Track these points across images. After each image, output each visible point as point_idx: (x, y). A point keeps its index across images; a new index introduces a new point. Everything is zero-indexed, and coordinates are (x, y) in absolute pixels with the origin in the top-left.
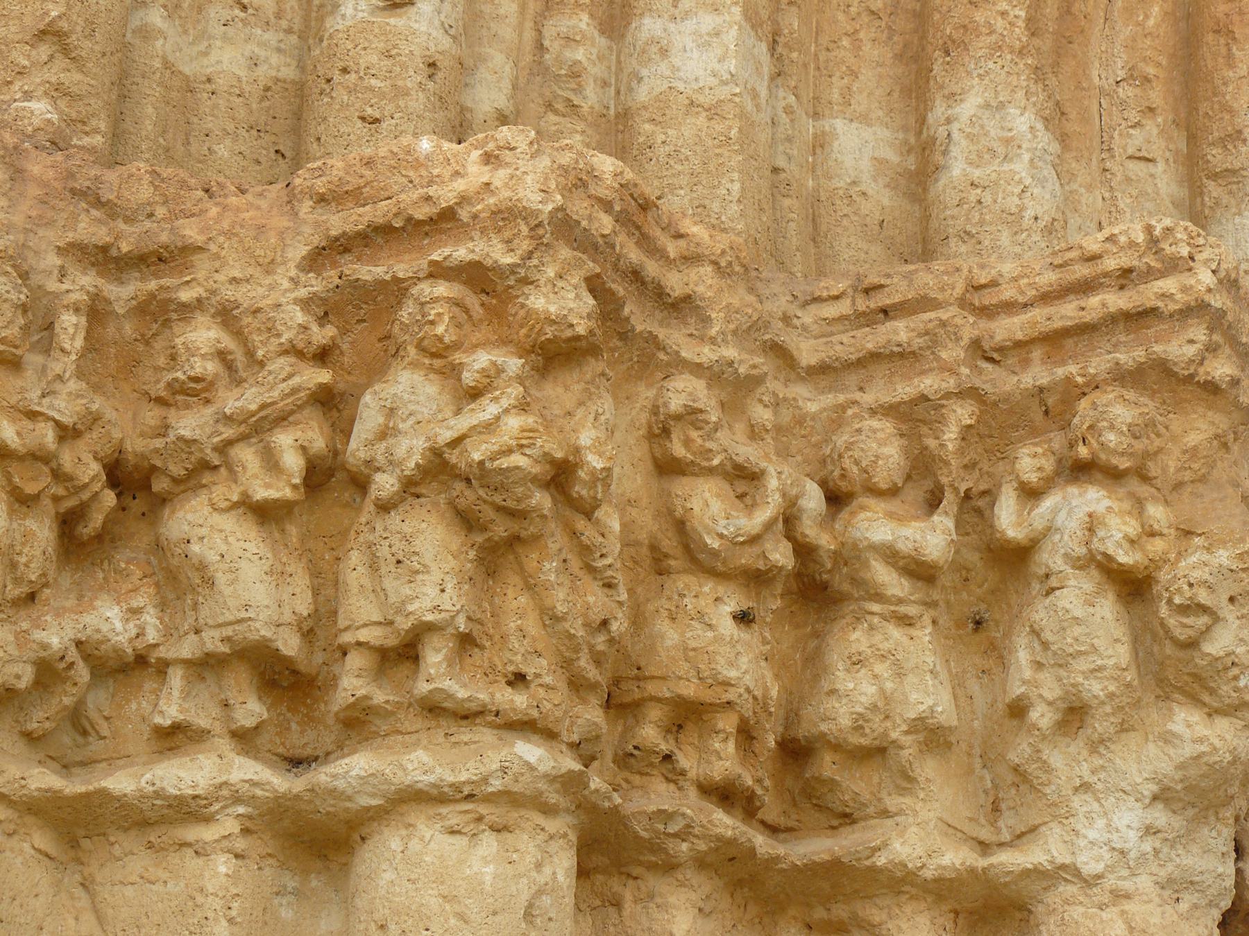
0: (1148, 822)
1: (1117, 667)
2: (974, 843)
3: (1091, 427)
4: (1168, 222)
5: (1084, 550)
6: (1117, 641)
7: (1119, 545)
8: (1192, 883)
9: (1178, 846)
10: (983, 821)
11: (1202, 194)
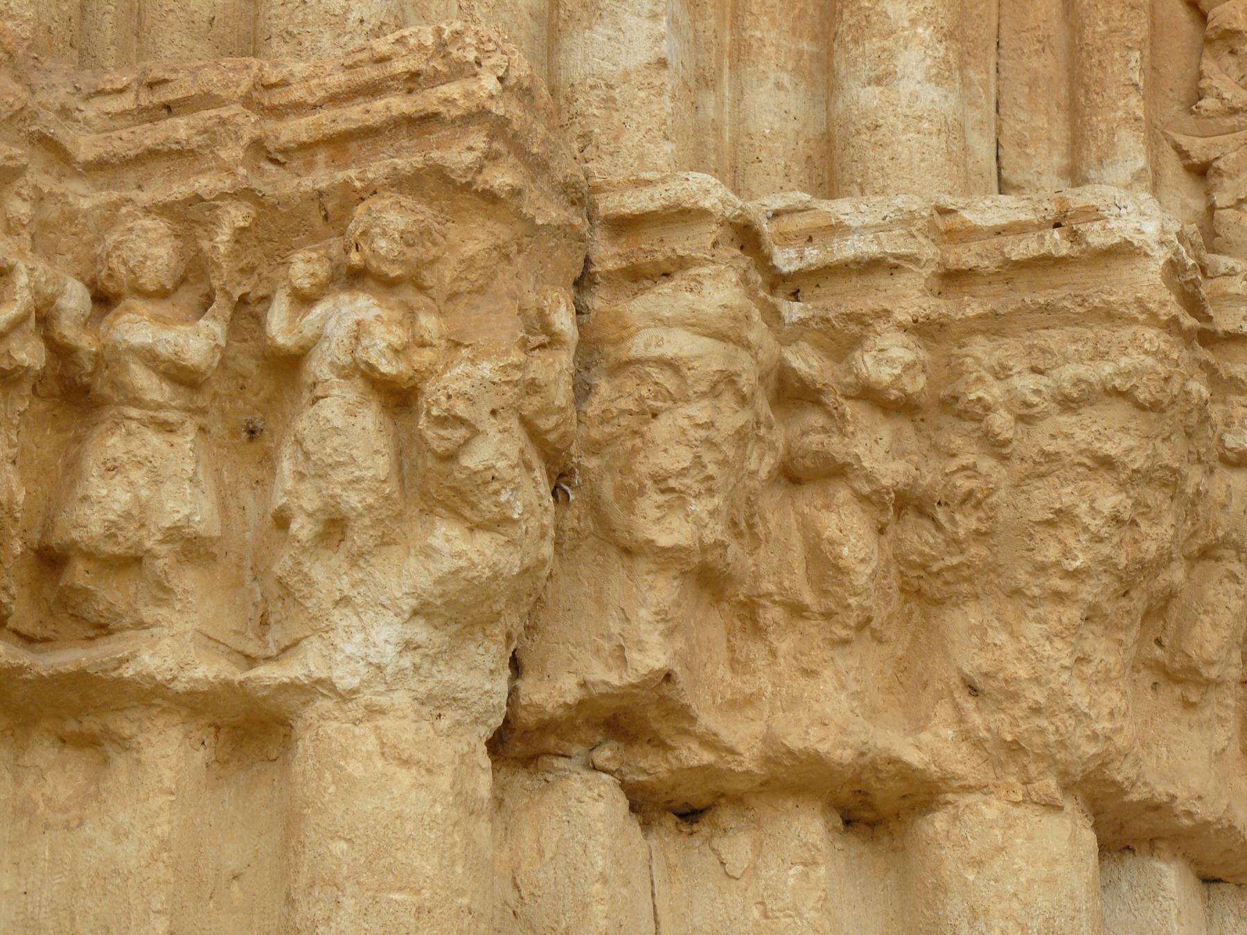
0: (407, 637)
1: (375, 478)
2: (239, 657)
3: (364, 233)
4: (458, 25)
5: (349, 359)
6: (377, 452)
7: (382, 354)
8: (455, 699)
9: (440, 662)
10: (250, 634)
11: (558, 6)
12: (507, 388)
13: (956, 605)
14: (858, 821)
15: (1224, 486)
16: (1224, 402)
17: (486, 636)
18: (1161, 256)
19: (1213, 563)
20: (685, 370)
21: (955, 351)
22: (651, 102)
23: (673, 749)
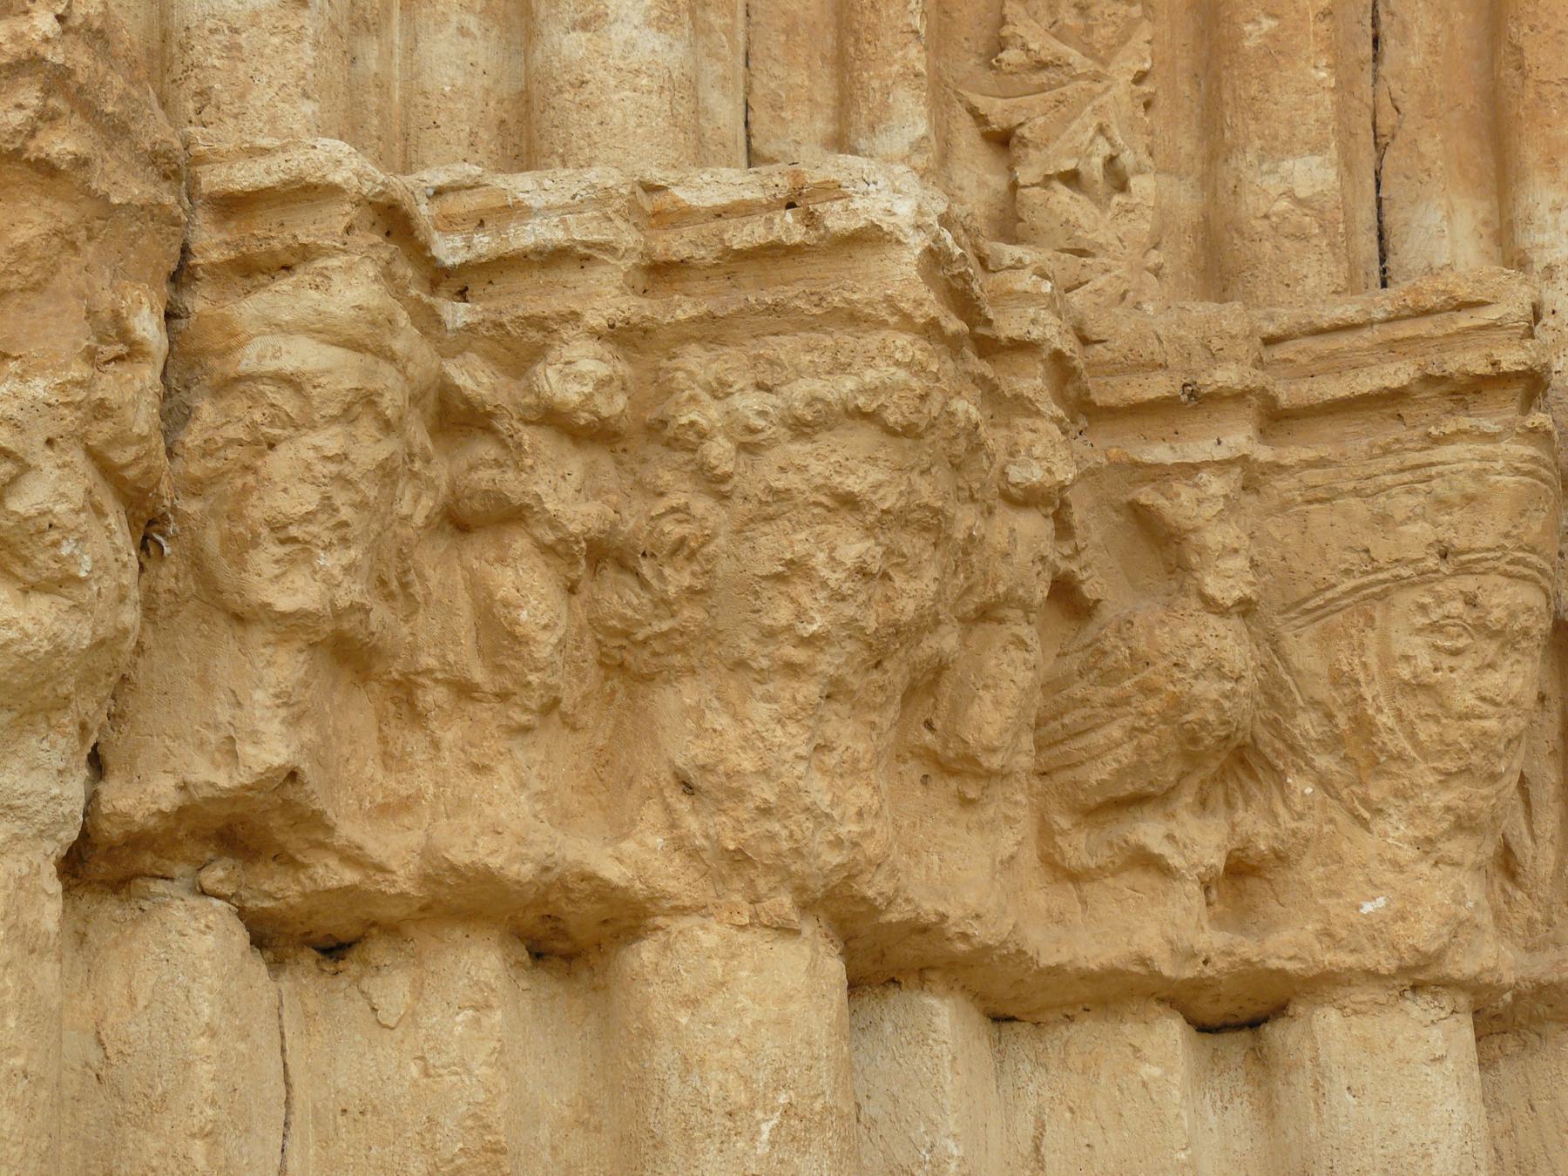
8: (10, 807)
12: (66, 412)
13: (668, 681)
14: (552, 952)
15: (1006, 531)
16: (1008, 426)
17: (50, 727)
18: (917, 243)
19: (995, 626)
20: (309, 388)
21: (664, 363)
22: (286, 50)
23: (305, 866)
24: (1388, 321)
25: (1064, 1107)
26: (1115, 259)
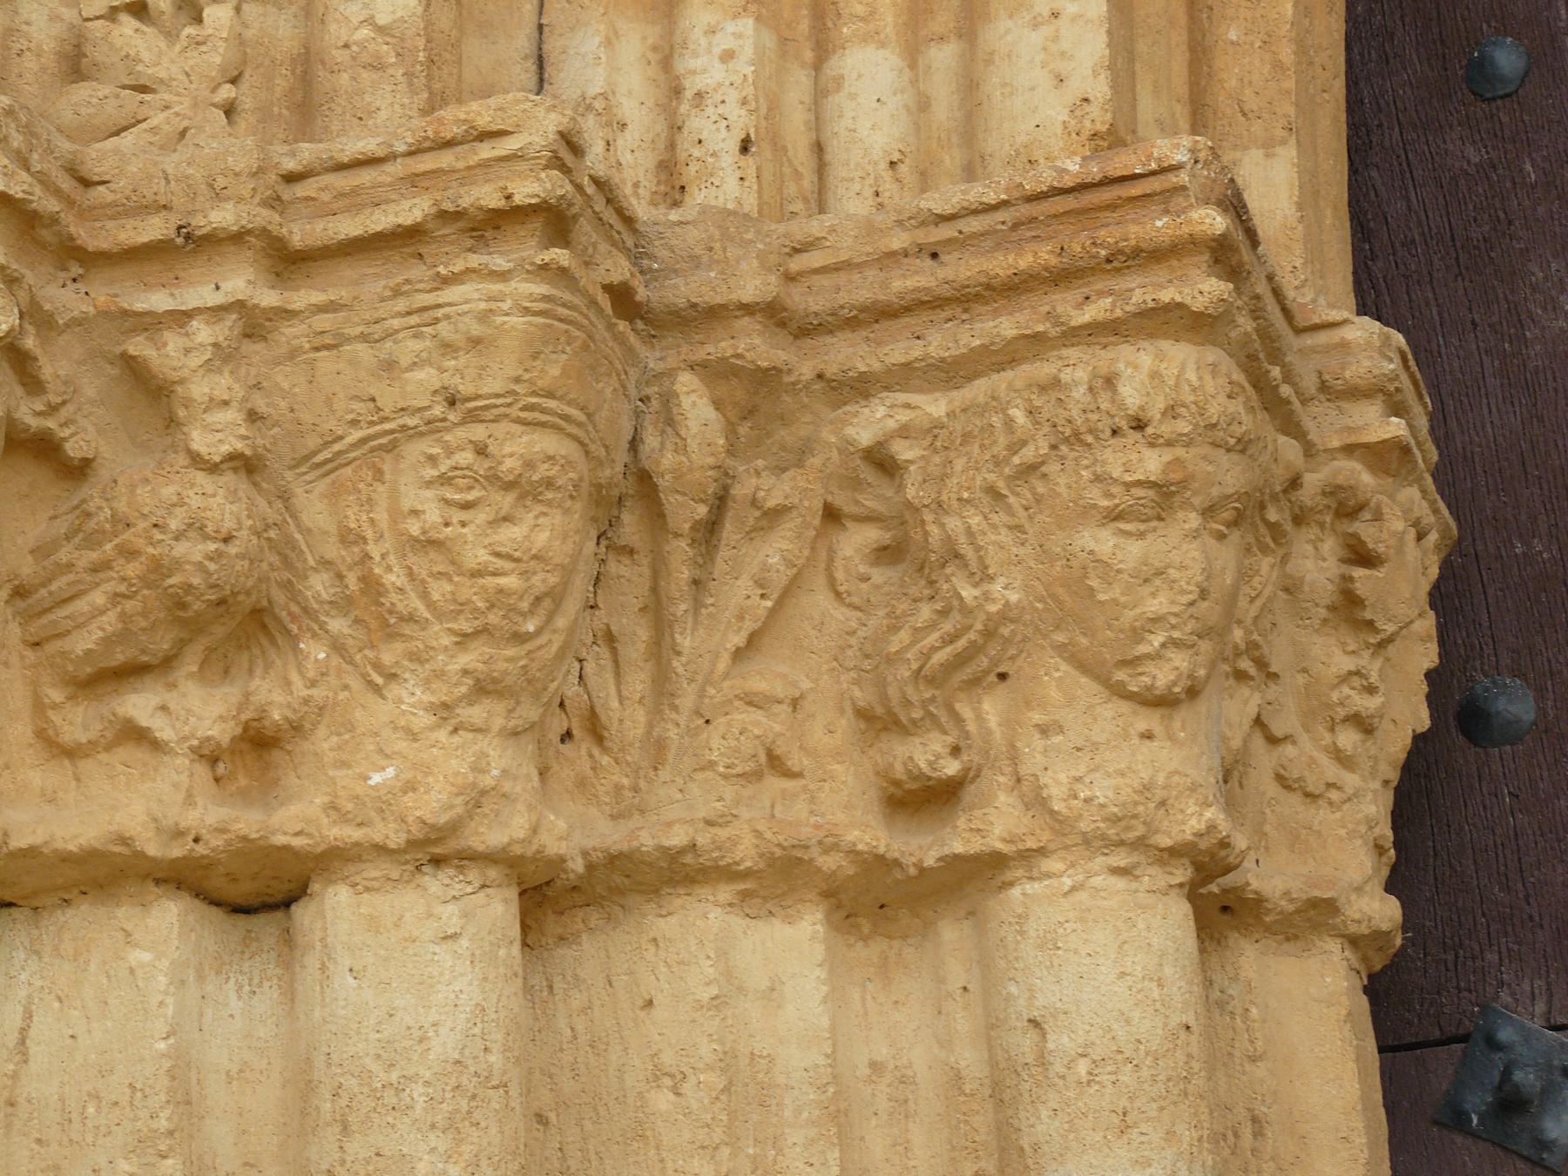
24: (410, 154)
25: (53, 996)
26: (178, 94)
